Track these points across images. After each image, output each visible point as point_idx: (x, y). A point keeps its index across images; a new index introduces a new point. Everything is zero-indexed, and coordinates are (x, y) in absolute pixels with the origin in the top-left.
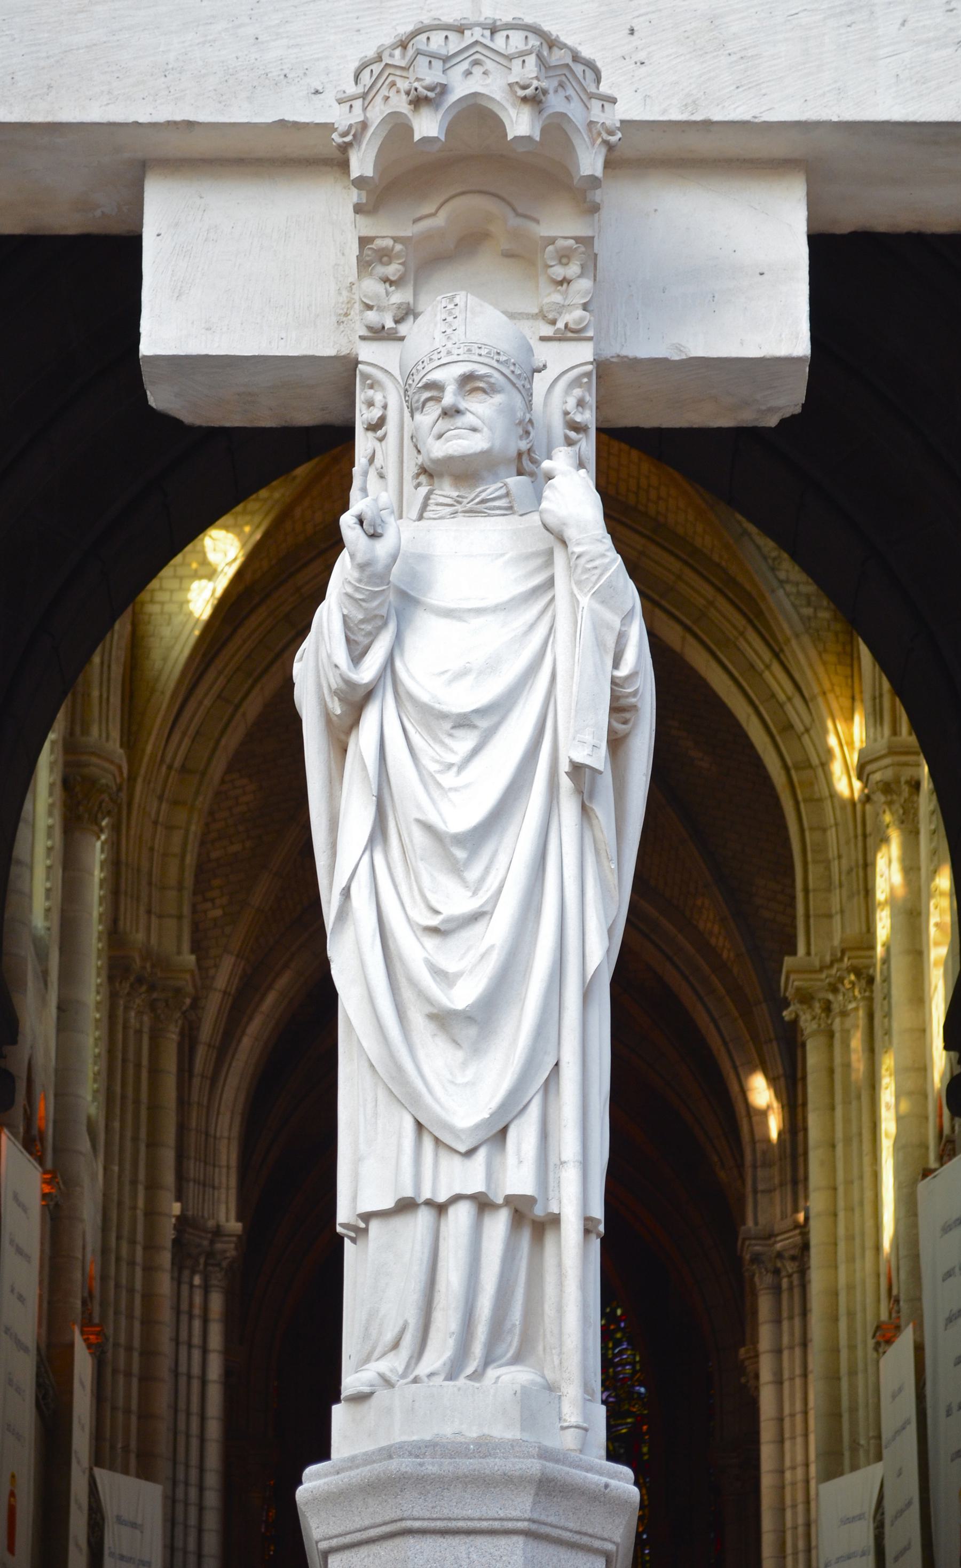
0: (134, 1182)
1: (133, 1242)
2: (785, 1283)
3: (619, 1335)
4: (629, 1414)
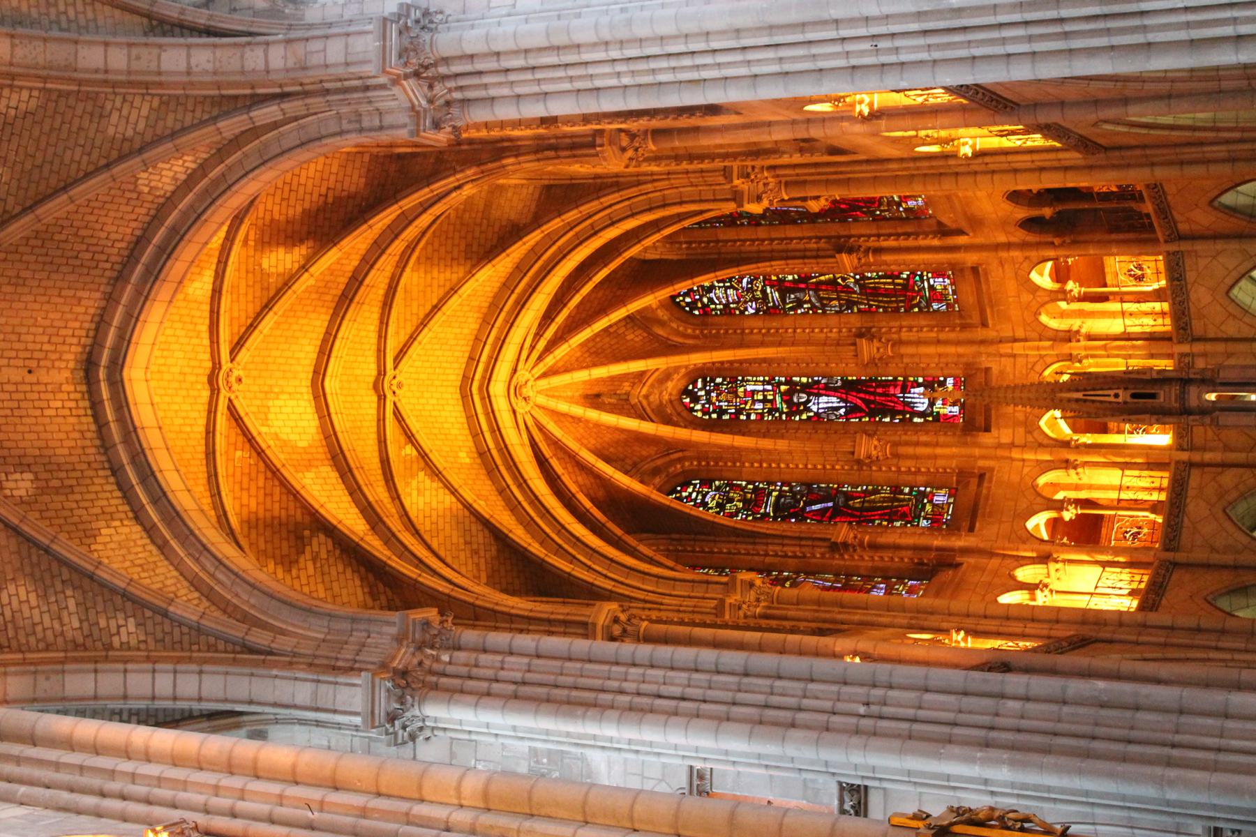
0: (57, 766)
1: (112, 774)
2: (457, 95)
3: (705, 300)
4: (764, 292)
